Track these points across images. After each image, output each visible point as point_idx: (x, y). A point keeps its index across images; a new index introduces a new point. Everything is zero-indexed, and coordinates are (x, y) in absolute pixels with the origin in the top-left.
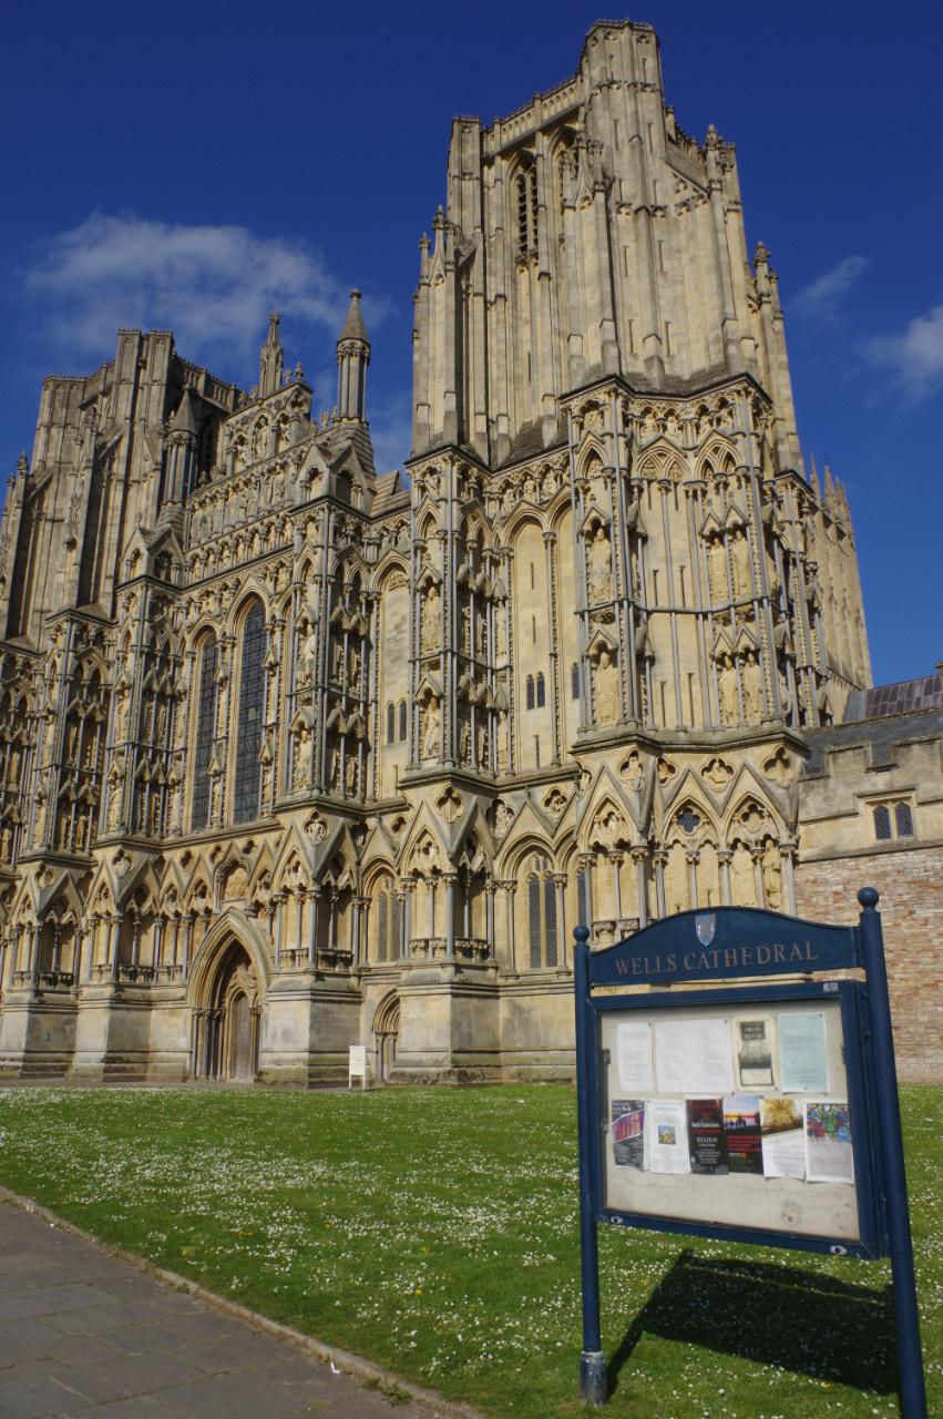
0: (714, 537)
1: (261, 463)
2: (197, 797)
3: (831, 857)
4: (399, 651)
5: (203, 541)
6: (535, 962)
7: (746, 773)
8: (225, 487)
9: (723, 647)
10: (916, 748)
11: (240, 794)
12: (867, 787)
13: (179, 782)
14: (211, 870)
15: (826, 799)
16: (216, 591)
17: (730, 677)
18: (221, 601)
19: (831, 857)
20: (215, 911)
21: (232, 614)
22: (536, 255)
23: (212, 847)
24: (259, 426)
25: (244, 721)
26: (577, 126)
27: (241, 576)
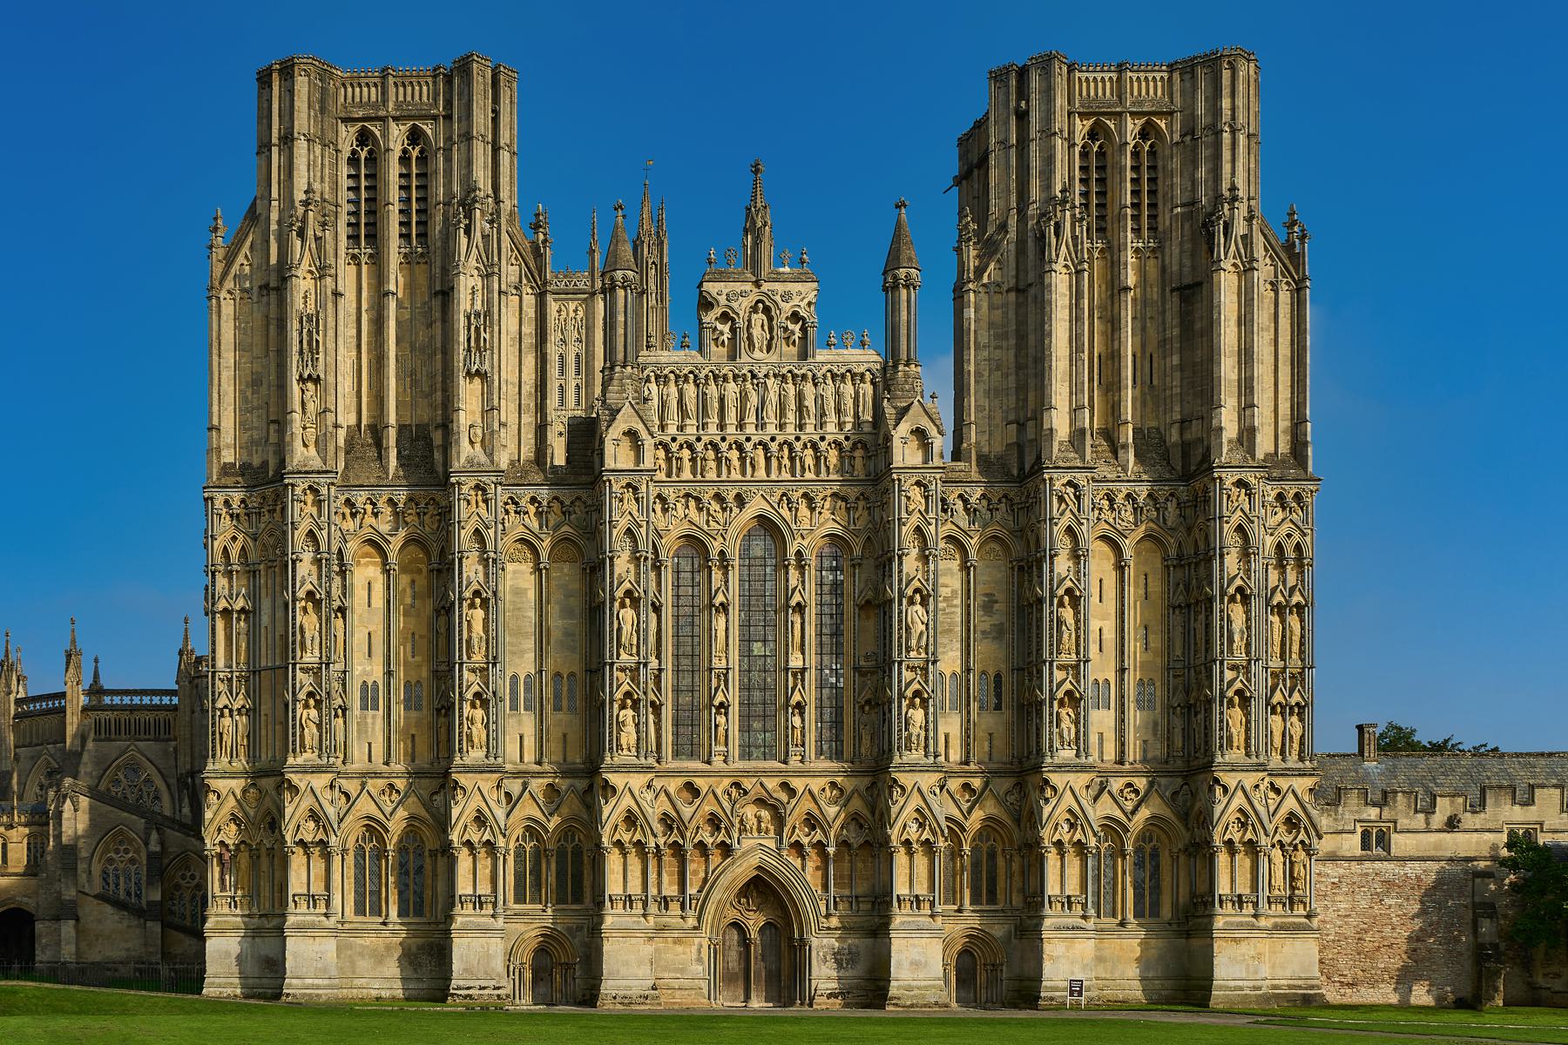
0: (1280, 610)
2: (677, 723)
3: (1333, 858)
5: (672, 430)
7: (1291, 795)
9: (1278, 697)
10: (1400, 794)
11: (745, 728)
12: (1364, 816)
13: (656, 708)
14: (726, 805)
15: (1336, 820)
16: (706, 498)
17: (1276, 722)
18: (708, 509)
19: (1333, 858)
23: (727, 782)
24: (754, 309)
25: (746, 653)
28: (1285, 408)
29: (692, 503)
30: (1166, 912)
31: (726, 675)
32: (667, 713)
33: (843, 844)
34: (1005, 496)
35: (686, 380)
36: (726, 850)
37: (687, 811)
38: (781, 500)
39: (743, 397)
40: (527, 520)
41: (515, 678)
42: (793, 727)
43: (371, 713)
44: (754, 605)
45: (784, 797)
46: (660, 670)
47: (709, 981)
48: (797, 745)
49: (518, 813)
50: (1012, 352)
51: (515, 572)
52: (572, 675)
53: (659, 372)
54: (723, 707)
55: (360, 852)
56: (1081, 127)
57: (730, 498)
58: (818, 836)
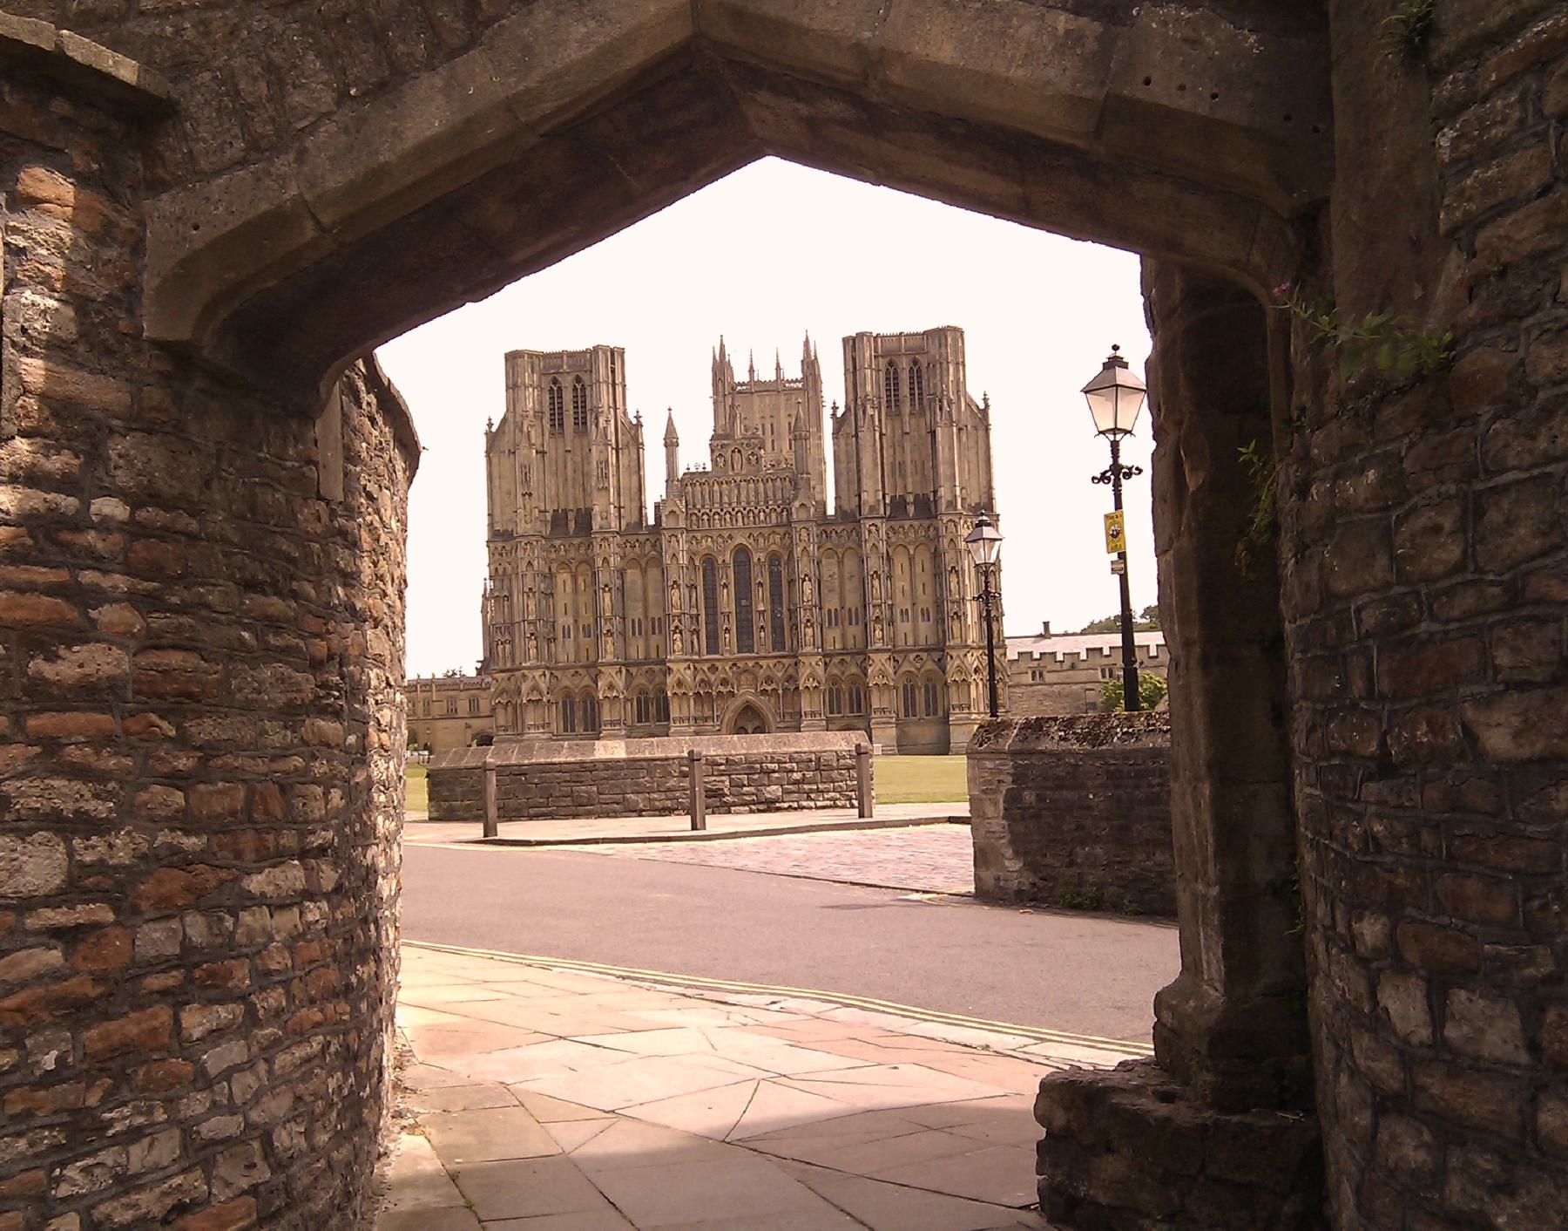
1: (737, 474)
3: (1018, 685)
5: (699, 506)
6: (906, 715)
13: (697, 632)
14: (731, 674)
19: (1018, 685)
22: (899, 414)
23: (730, 663)
24: (733, 452)
26: (923, 360)
27: (734, 533)
28: (983, 482)
30: (940, 713)
36: (732, 694)
37: (713, 678)
38: (749, 537)
39: (730, 491)
41: (633, 620)
43: (567, 639)
49: (636, 682)
52: (659, 619)
55: (565, 704)
56: (883, 363)
58: (774, 686)
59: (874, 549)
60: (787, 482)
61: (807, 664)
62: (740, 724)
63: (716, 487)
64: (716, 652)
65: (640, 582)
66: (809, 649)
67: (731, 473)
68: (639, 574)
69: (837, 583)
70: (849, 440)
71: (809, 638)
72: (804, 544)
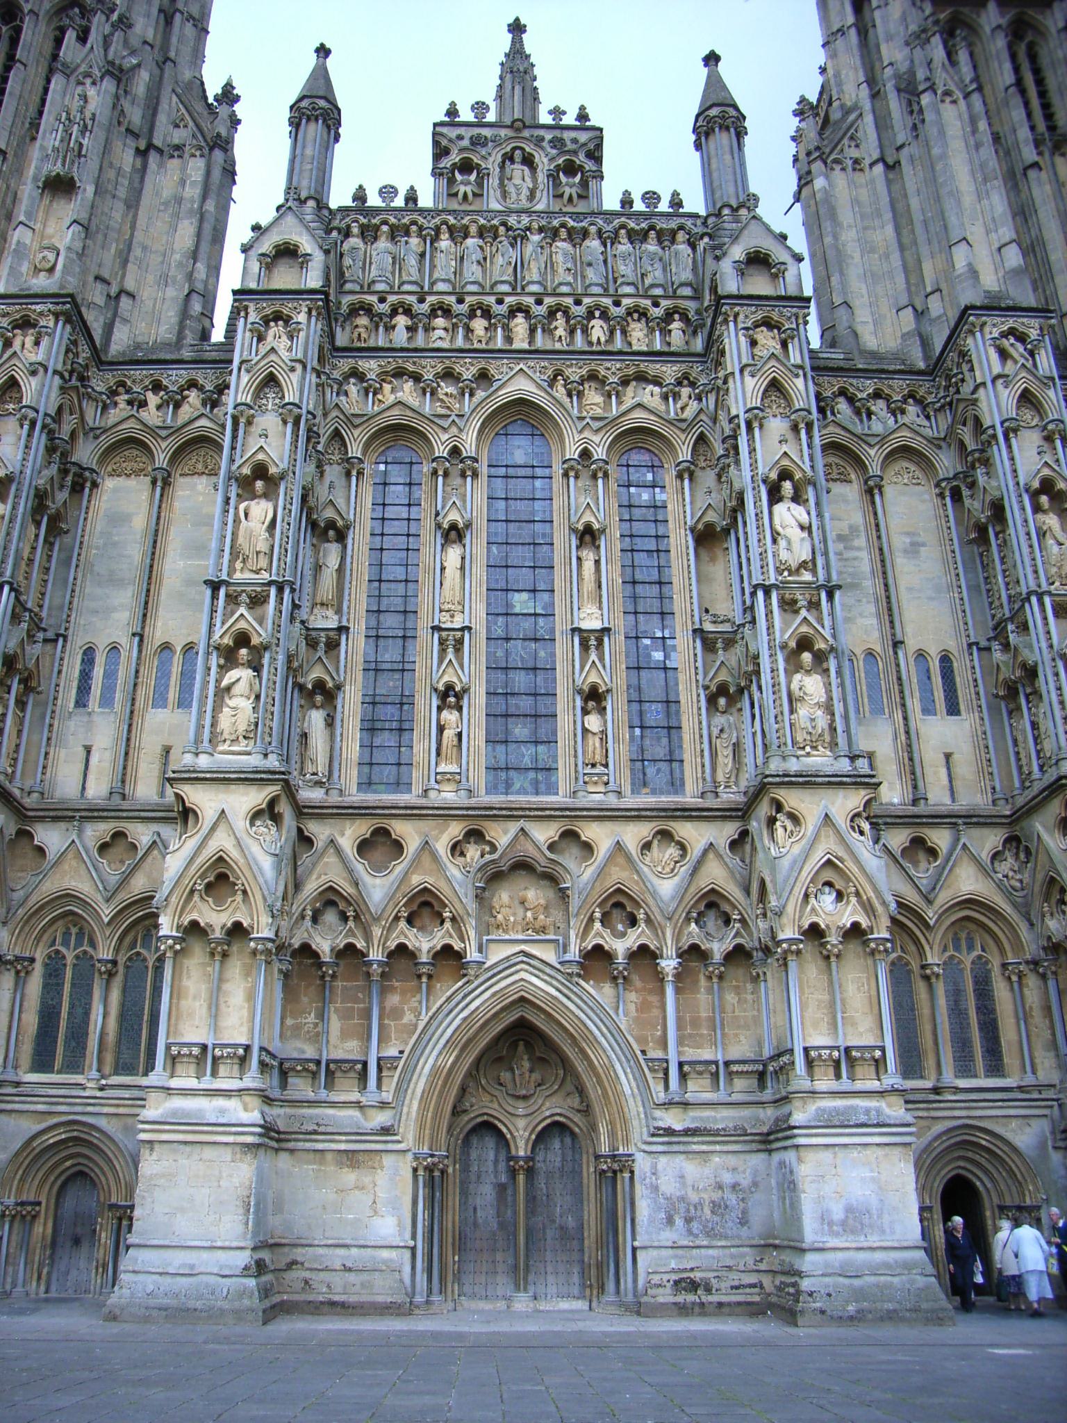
2: (371, 728)
4: (852, 575)
8: (437, 220)
13: (325, 694)
14: (454, 872)
16: (428, 375)
20: (472, 955)
21: (476, 424)
23: (456, 830)
24: (509, 157)
25: (500, 612)
29: (409, 385)
31: (459, 644)
32: (351, 702)
33: (693, 954)
34: (911, 395)
35: (407, 234)
38: (552, 382)
40: (143, 414)
41: (89, 656)
42: (585, 731)
44: (514, 535)
45: (569, 859)
46: (343, 629)
47: (413, 1250)
48: (593, 765)
50: (889, 230)
51: (115, 490)
53: (363, 221)
54: (450, 696)
57: (467, 375)
59: (1028, 415)
60: (683, 248)
61: (811, 821)
62: (484, 1105)
63: (445, 243)
64: (400, 784)
65: (140, 523)
66: (820, 760)
67: (495, 206)
68: (145, 495)
69: (864, 561)
70: (860, 178)
71: (810, 715)
72: (772, 370)
